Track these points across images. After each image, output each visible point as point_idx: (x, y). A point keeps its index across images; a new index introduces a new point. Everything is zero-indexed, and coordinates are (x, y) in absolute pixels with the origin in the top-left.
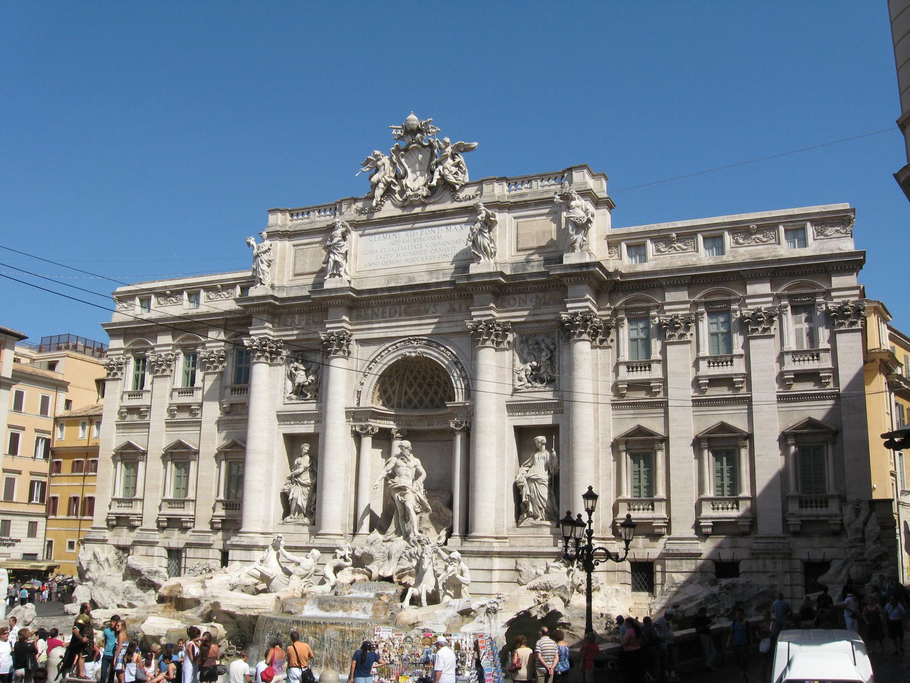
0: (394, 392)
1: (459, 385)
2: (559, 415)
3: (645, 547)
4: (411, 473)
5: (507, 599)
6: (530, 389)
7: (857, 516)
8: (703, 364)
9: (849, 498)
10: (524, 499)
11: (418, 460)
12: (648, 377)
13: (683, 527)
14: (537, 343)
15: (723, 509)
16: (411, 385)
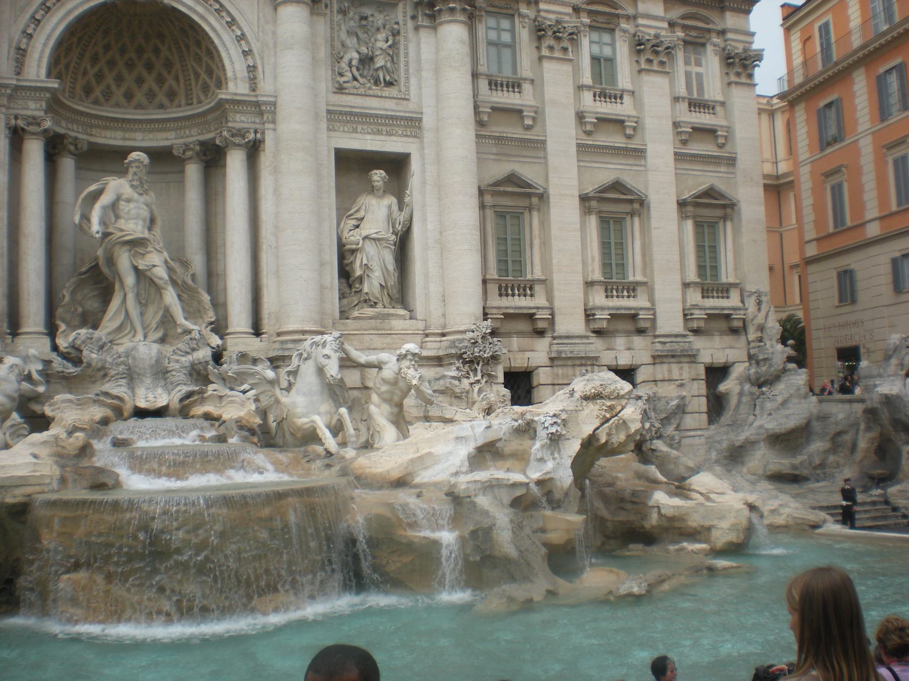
0: (67, 67)
1: (234, 63)
2: (411, 140)
3: (522, 350)
4: (145, 213)
5: (564, 416)
6: (362, 91)
7: (759, 310)
8: (588, 96)
9: (751, 287)
10: (358, 272)
11: (152, 194)
12: (519, 102)
13: (571, 322)
14: (366, 18)
15: (618, 297)
16: (95, 59)
